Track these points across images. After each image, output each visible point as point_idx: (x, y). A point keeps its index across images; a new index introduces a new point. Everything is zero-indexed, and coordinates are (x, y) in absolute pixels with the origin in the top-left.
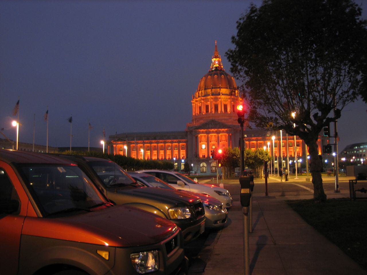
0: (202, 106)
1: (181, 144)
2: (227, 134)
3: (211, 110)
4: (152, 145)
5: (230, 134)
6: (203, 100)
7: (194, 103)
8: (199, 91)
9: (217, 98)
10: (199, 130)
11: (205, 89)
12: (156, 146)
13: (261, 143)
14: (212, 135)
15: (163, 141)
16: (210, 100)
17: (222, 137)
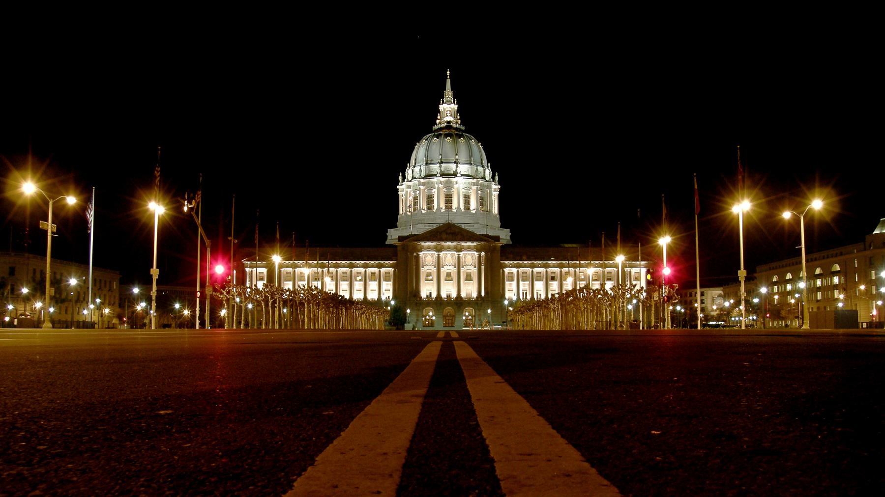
1: (383, 270)
2: (476, 254)
3: (439, 203)
4: (297, 270)
6: (423, 184)
7: (403, 190)
9: (451, 182)
10: (423, 243)
11: (427, 164)
15: (348, 262)
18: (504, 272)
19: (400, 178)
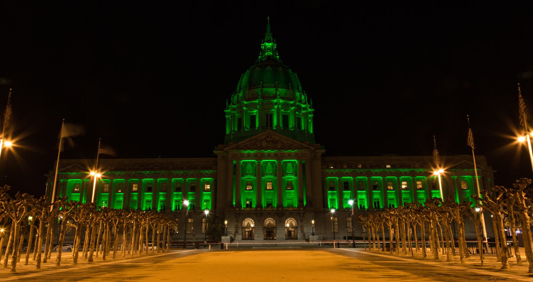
6: (246, 106)
8: (239, 92)
16: (258, 107)
17: (286, 166)
19: (227, 105)
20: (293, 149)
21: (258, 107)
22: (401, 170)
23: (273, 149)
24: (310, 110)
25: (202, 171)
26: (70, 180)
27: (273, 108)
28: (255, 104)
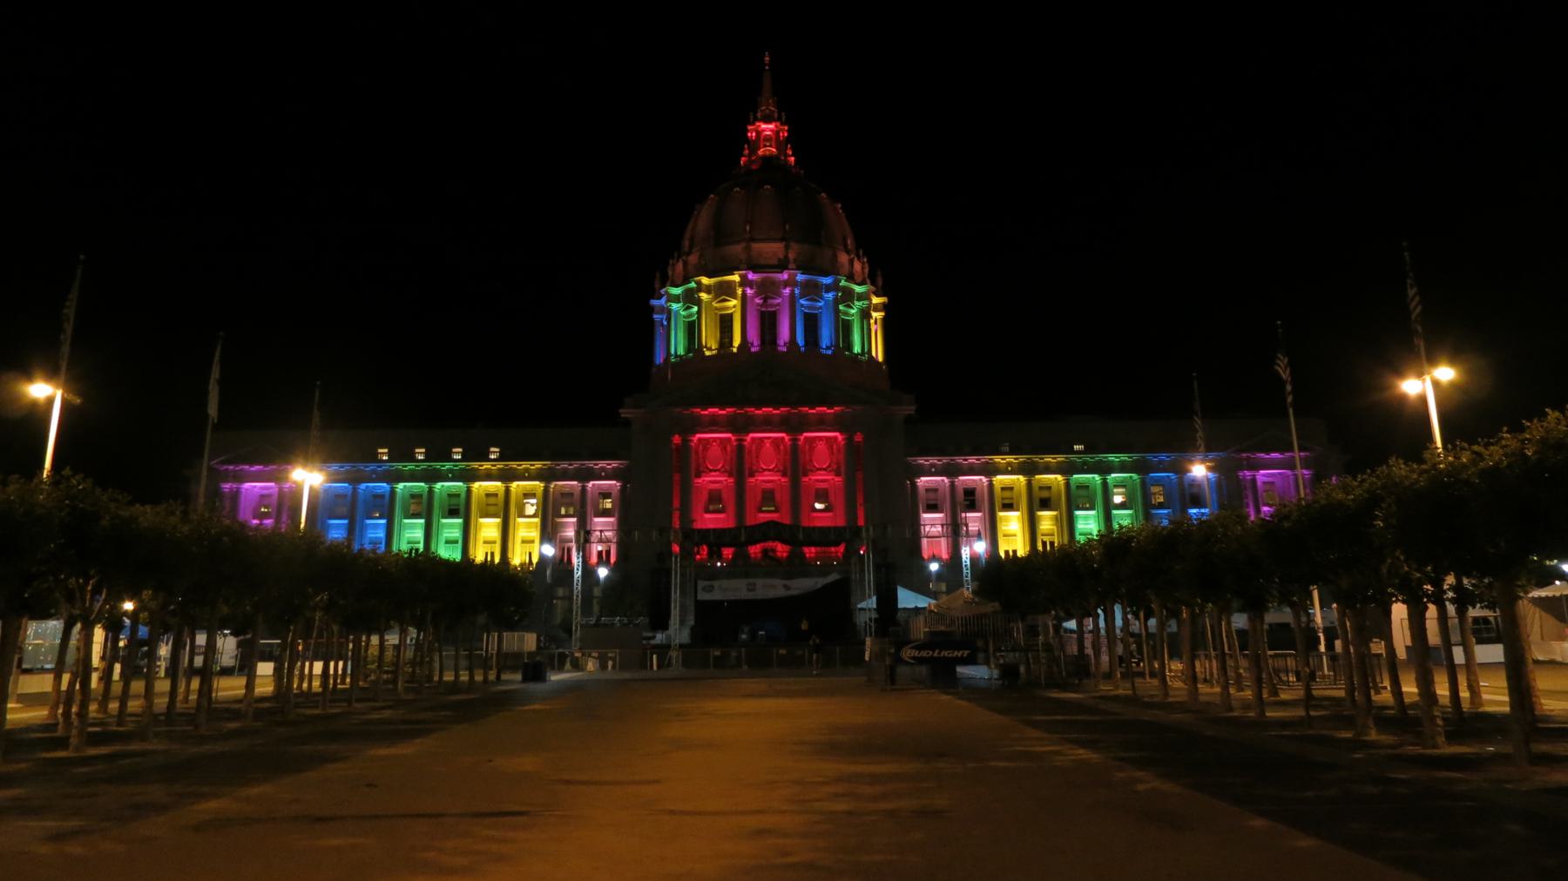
0: (699, 318)
5: (858, 438)
6: (708, 290)
8: (689, 254)
12: (458, 496)
13: (1011, 489)
14: (762, 439)
16: (739, 291)
17: (812, 449)
18: (914, 485)
20: (830, 406)
21: (739, 291)
22: (1112, 457)
23: (776, 406)
24: (876, 300)
25: (590, 464)
26: (247, 485)
27: (780, 295)
28: (731, 284)
